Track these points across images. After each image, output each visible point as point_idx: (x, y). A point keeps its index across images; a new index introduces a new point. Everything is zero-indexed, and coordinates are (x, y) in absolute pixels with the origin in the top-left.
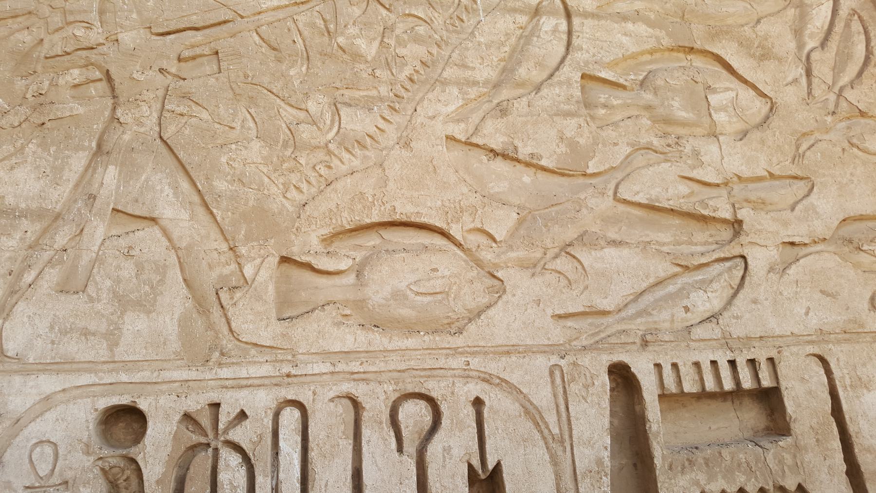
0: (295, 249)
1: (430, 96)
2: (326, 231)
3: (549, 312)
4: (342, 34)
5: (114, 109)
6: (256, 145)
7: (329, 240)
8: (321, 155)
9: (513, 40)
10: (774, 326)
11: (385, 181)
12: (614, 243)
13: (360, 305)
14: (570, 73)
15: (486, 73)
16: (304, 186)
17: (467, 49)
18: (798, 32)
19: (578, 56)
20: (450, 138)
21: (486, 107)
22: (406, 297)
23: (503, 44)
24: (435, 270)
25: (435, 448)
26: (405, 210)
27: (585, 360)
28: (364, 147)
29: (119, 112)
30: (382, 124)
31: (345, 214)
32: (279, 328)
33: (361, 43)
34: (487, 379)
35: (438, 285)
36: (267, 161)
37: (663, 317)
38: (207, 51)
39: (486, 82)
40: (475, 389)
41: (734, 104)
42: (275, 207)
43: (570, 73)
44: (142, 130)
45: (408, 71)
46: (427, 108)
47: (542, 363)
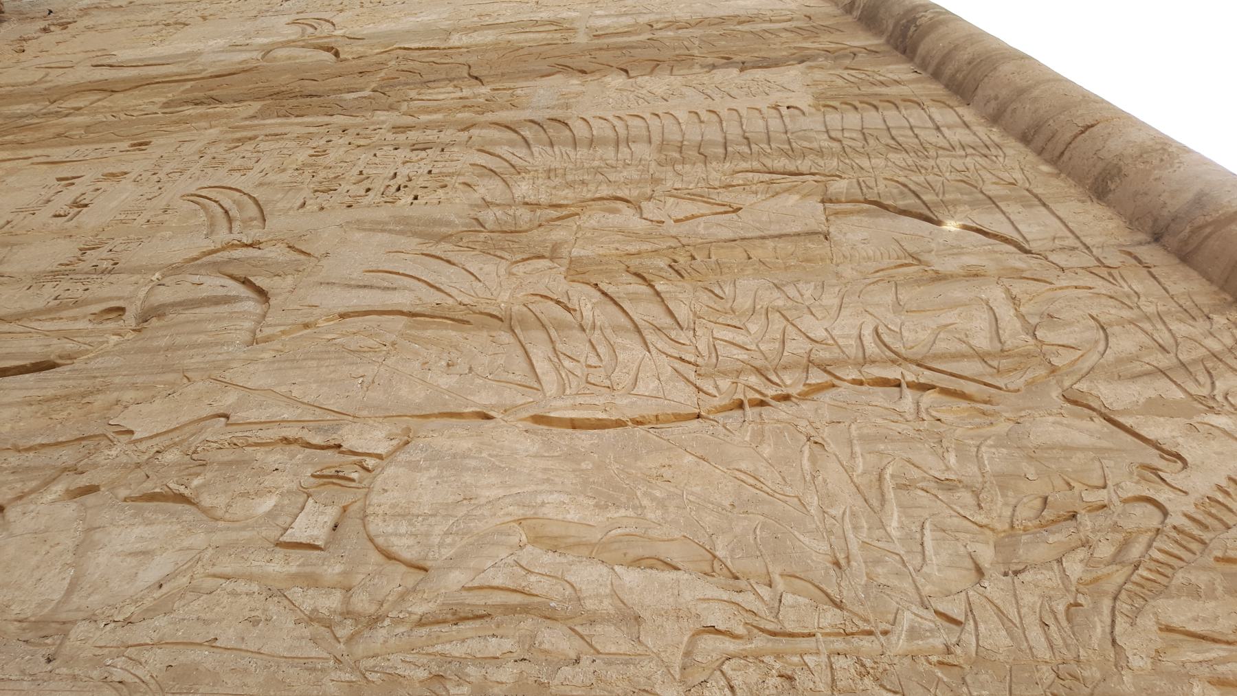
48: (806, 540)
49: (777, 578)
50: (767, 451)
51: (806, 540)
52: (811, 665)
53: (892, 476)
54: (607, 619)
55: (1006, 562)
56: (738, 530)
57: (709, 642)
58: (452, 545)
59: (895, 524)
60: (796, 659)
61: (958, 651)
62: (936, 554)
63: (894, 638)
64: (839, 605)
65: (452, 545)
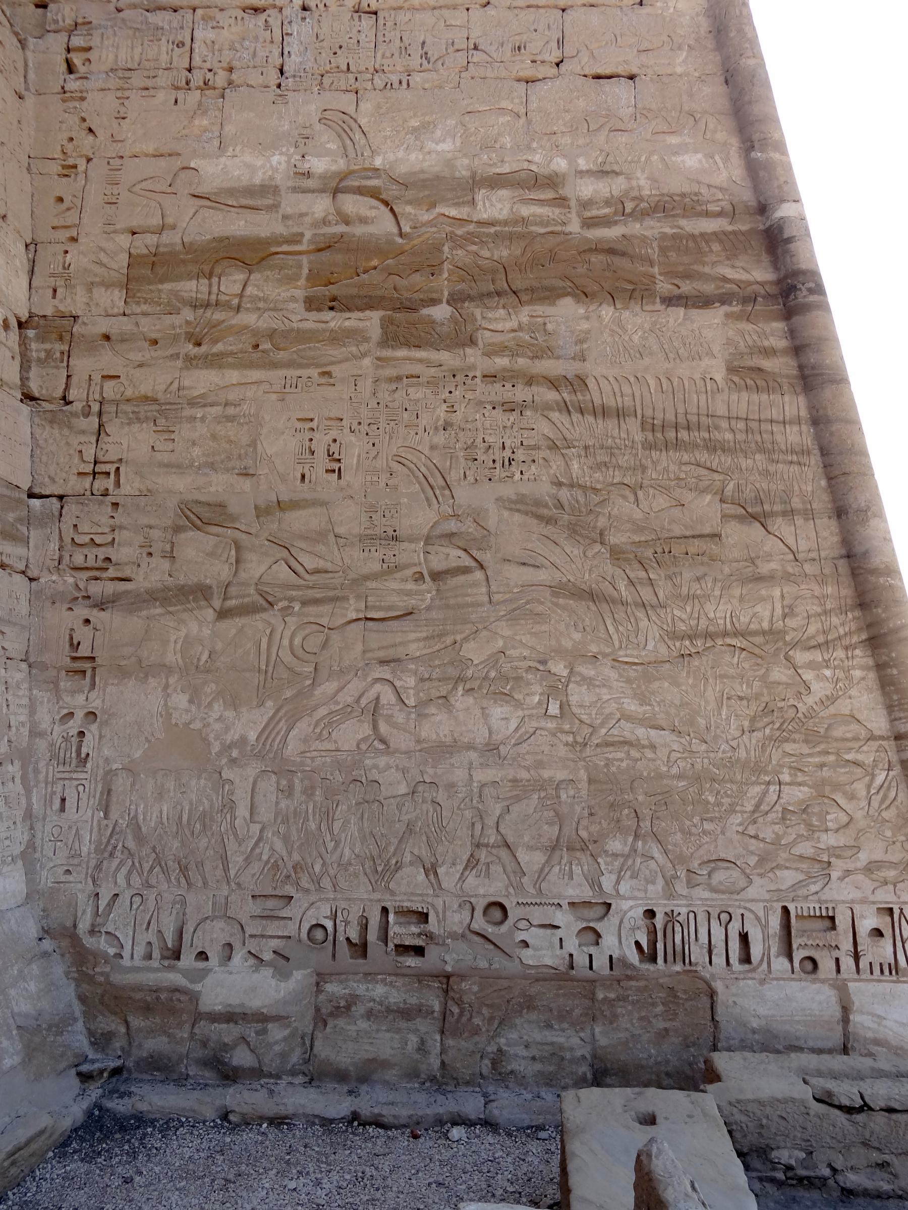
6: (679, 834)
10: (837, 897)
11: (716, 847)
12: (787, 868)
13: (709, 885)
14: (778, 808)
15: (749, 808)
18: (869, 787)
19: (782, 801)
25: (730, 926)
26: (723, 855)
27: (775, 904)
33: (710, 798)
34: (745, 908)
35: (732, 880)
37: (800, 893)
40: (742, 911)
41: (836, 818)
43: (778, 808)
46: (731, 820)
47: (762, 905)
50: (690, 681)
57: (673, 755)
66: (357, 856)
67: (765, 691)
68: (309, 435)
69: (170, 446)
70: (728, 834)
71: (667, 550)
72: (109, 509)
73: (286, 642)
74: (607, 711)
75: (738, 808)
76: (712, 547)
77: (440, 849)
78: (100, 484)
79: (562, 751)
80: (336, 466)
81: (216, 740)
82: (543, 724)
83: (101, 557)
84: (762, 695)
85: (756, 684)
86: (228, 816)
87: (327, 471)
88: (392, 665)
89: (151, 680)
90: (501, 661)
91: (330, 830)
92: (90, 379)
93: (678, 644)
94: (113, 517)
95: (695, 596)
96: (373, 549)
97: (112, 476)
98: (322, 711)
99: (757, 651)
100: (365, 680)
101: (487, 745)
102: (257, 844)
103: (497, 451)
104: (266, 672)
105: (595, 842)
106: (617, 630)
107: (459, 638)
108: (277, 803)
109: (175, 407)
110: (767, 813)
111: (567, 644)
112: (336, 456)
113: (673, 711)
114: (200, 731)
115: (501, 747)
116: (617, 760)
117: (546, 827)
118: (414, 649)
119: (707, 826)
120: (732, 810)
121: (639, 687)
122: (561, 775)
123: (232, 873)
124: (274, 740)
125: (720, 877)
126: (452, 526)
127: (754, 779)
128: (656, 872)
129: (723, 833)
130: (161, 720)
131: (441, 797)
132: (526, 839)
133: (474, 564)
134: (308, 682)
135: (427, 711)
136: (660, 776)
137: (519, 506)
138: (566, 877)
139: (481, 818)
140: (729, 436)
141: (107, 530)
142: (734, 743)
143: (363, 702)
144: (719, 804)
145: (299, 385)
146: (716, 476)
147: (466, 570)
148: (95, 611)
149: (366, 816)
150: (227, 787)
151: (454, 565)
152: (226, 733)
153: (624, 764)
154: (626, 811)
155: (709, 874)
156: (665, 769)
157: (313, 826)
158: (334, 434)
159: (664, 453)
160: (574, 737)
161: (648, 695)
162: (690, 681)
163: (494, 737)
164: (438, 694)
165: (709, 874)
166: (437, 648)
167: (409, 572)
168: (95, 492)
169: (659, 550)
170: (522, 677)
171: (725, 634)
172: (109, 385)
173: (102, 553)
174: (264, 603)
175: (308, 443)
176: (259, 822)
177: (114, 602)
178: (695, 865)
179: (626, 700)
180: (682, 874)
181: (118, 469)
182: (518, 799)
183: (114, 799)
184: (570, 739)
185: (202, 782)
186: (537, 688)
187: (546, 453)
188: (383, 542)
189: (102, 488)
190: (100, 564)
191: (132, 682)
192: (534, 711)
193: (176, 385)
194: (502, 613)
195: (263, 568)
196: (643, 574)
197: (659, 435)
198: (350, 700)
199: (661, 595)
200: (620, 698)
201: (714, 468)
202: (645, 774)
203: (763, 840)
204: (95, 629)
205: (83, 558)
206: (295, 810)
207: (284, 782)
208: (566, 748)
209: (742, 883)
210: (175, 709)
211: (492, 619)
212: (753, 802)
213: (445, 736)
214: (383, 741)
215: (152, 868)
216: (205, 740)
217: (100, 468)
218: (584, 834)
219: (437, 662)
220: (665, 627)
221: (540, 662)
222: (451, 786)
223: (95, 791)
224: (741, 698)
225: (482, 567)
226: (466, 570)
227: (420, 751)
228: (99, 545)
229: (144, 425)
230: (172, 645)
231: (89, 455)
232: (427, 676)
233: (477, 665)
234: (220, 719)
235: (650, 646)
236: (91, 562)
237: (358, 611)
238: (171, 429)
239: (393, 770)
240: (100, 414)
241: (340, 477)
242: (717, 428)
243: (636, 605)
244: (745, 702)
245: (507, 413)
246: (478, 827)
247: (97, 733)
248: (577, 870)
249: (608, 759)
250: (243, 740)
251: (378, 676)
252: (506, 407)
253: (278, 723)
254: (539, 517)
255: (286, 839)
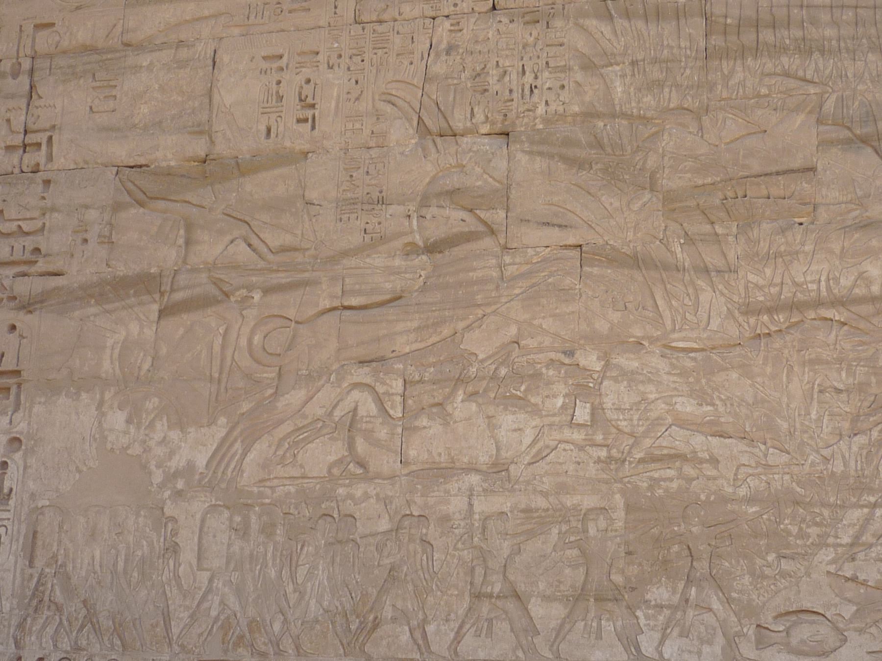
0: (762, 622)
1: (821, 552)
2: (774, 614)
3: (865, 650)
4: (783, 524)
5: (692, 562)
6: (747, 577)
7: (776, 618)
8: (773, 581)
9: (861, 522)
11: (799, 592)
13: (788, 644)
15: (846, 540)
16: (766, 595)
17: (839, 528)
20: (828, 572)
21: (846, 556)
22: (806, 642)
23: (855, 525)
24: (818, 631)
26: (807, 605)
28: (791, 576)
29: (695, 563)
30: (799, 566)
31: (782, 607)
32: (757, 652)
35: (819, 638)
36: (751, 584)
38: (726, 534)
39: (847, 544)
42: (754, 604)
44: (704, 571)
45: (811, 540)
48: (779, 421)
49: (768, 441)
51: (779, 421)
52: (776, 478)
53: (818, 385)
54: (707, 461)
55: (853, 429)
56: (755, 417)
58: (643, 425)
59: (815, 413)
60: (771, 476)
61: (825, 472)
62: (827, 427)
63: (804, 466)
64: (788, 453)
65: (643, 425)
66: (326, 611)
67: (873, 379)
68: (276, 77)
69: (111, 104)
70: (814, 576)
71: (740, 194)
72: (40, 188)
73: (243, 342)
74: (653, 415)
75: (831, 540)
76: (804, 186)
77: (431, 600)
78: (30, 159)
79: (592, 470)
80: (309, 113)
81: (158, 466)
82: (567, 434)
83: (29, 248)
84: (869, 384)
85: (861, 370)
86: (171, 563)
87: (299, 121)
88: (374, 364)
89: (84, 395)
90: (514, 355)
91: (293, 578)
92: (21, 31)
93: (752, 320)
94: (44, 198)
95: (778, 255)
96: (353, 216)
97: (44, 147)
98: (286, 428)
99: (862, 325)
100: (339, 386)
101: (494, 465)
102: (204, 598)
103: (514, 76)
104: (219, 381)
105: (633, 589)
106: (671, 307)
107: (461, 325)
108: (229, 545)
109: (118, 55)
110: (871, 546)
111: (602, 326)
112: (310, 100)
113: (744, 410)
114: (139, 456)
115: (512, 468)
116: (664, 480)
117: (567, 571)
118: (404, 345)
119: (785, 565)
120: (821, 544)
121: (698, 381)
122: (589, 502)
123: (175, 631)
124: (228, 465)
125: (803, 633)
126: (455, 181)
127: (854, 500)
128: (714, 629)
129: (808, 574)
130: (94, 445)
131: (432, 532)
132: (542, 586)
133: (481, 228)
134: (270, 391)
135: (417, 423)
136: (724, 500)
137: (544, 148)
138: (593, 636)
139: (484, 560)
140: (829, 32)
141: (36, 214)
142: (826, 452)
143: (338, 413)
144: (802, 535)
145: (266, 13)
146: (812, 90)
147: (470, 237)
148: (22, 315)
149: (338, 559)
150: (170, 526)
151: (455, 230)
152: (170, 459)
153: (674, 485)
154: (675, 548)
155: (788, 631)
156: (730, 490)
157: (273, 573)
158: (306, 72)
159: (739, 62)
160: (609, 451)
161: (709, 391)
162: (769, 370)
163: (503, 454)
164: (432, 401)
165: (788, 631)
166: (431, 341)
167: (398, 244)
168: (25, 169)
169: (730, 194)
170: (541, 374)
171: (819, 303)
172: (43, 34)
173: (29, 243)
174: (217, 293)
175: (274, 86)
176: (207, 570)
177: (42, 302)
178: (767, 619)
179: (679, 399)
180: (750, 631)
181: (50, 139)
182: (531, 534)
183: (39, 543)
184: (603, 453)
185: (141, 519)
186: (561, 388)
187: (579, 76)
188: (366, 207)
189: (33, 163)
190: (28, 256)
191: (62, 400)
192: (557, 419)
193: (119, 29)
194: (517, 291)
195: (220, 248)
196: (708, 228)
197: (733, 38)
198: (320, 412)
199: (731, 256)
200: (671, 396)
201: (808, 77)
202: (703, 497)
203: (864, 583)
204: (22, 337)
205: (8, 249)
206: (251, 555)
207: (238, 519)
208: (598, 466)
209: (832, 640)
210: (111, 430)
211: (504, 300)
212: (851, 532)
213: (440, 454)
214: (361, 464)
215: (82, 627)
216: (144, 467)
217: (31, 138)
218: (618, 579)
219: (432, 360)
220: (736, 299)
221: (564, 353)
222: (446, 519)
223: (19, 532)
224: (839, 391)
225: (492, 232)
226: (470, 237)
227: (406, 475)
228: (27, 234)
229: (82, 81)
230: (108, 351)
231: (19, 121)
232: (417, 378)
233: (483, 361)
234: (164, 441)
235: (714, 326)
236: (17, 256)
237: (332, 297)
238: (112, 83)
239: (373, 501)
240: (32, 72)
241: (313, 128)
242: (814, 22)
243: (696, 269)
244: (844, 396)
245: (530, 27)
246: (479, 571)
247: (21, 463)
248: (608, 626)
249: (652, 479)
250: (190, 467)
251: (356, 379)
252: (528, 18)
253: (232, 445)
254: (565, 159)
255: (239, 591)
